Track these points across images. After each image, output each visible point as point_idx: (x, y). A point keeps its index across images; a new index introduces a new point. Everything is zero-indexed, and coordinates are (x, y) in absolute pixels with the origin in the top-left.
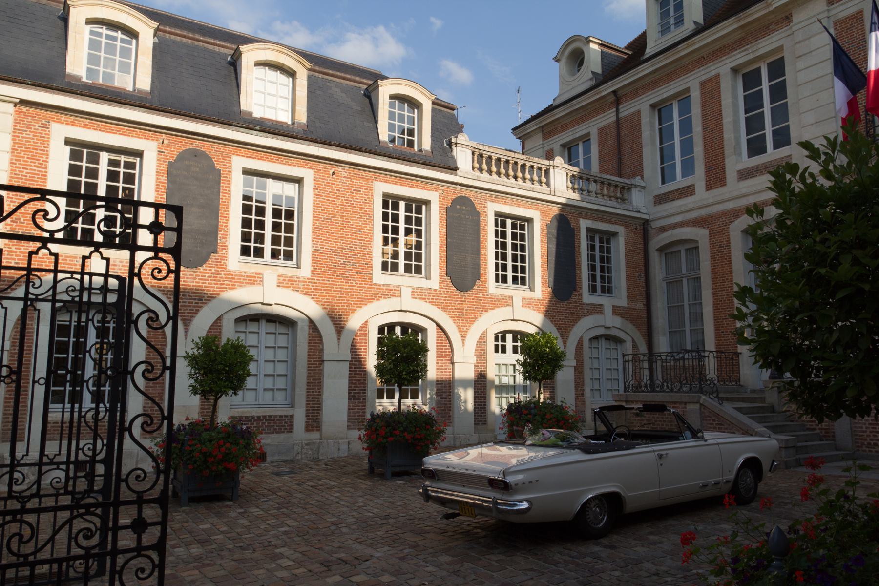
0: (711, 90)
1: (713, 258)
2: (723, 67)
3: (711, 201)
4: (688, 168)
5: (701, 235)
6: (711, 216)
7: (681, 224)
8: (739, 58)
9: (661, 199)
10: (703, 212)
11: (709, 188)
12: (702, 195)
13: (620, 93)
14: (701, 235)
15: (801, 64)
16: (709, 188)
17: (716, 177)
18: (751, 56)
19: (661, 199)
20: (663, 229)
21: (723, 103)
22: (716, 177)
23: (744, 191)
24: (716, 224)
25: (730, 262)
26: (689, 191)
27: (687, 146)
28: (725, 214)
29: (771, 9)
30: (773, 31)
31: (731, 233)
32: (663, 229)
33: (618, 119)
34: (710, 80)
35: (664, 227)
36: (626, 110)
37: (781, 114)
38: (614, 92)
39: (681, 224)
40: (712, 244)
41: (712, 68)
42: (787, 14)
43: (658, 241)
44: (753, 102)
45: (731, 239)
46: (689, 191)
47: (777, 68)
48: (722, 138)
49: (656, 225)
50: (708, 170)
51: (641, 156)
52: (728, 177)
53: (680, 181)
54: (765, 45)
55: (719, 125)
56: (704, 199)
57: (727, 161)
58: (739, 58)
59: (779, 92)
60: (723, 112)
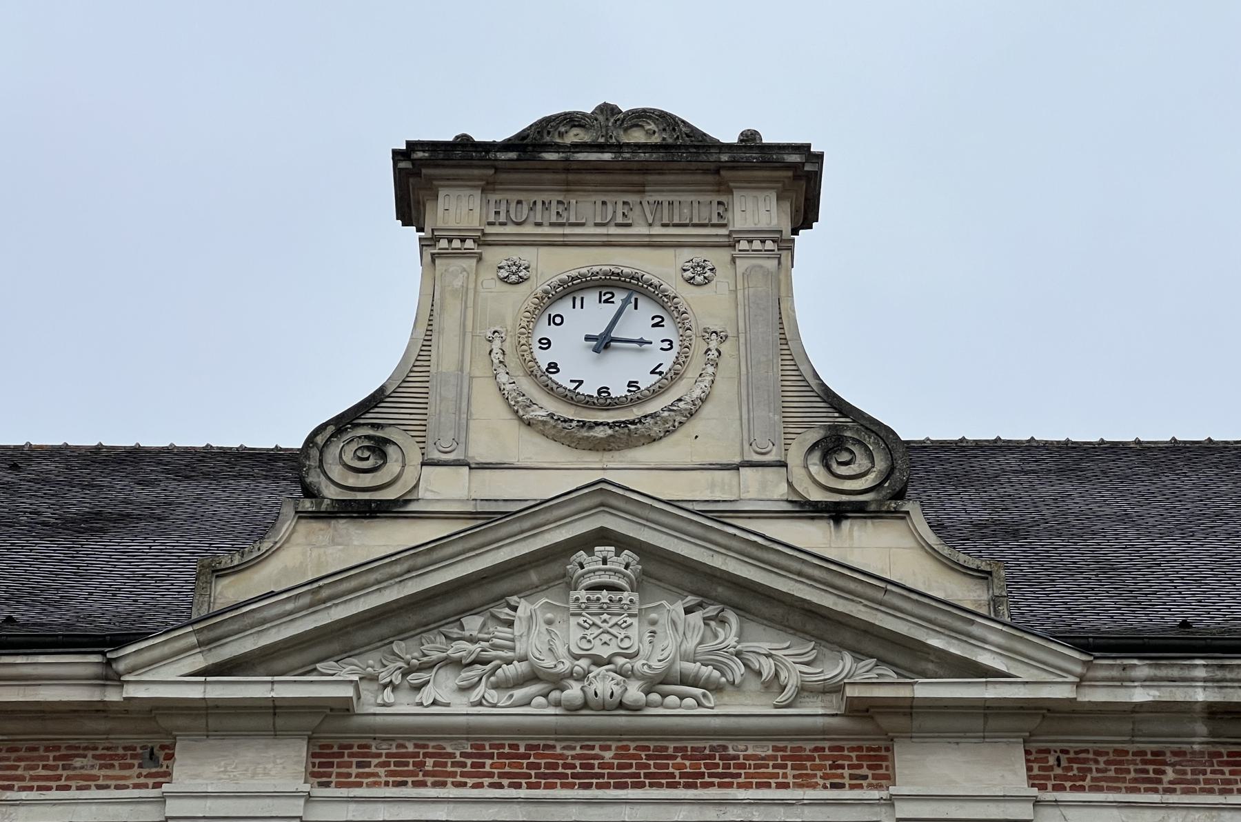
29: (113, 696)
42: (156, 742)
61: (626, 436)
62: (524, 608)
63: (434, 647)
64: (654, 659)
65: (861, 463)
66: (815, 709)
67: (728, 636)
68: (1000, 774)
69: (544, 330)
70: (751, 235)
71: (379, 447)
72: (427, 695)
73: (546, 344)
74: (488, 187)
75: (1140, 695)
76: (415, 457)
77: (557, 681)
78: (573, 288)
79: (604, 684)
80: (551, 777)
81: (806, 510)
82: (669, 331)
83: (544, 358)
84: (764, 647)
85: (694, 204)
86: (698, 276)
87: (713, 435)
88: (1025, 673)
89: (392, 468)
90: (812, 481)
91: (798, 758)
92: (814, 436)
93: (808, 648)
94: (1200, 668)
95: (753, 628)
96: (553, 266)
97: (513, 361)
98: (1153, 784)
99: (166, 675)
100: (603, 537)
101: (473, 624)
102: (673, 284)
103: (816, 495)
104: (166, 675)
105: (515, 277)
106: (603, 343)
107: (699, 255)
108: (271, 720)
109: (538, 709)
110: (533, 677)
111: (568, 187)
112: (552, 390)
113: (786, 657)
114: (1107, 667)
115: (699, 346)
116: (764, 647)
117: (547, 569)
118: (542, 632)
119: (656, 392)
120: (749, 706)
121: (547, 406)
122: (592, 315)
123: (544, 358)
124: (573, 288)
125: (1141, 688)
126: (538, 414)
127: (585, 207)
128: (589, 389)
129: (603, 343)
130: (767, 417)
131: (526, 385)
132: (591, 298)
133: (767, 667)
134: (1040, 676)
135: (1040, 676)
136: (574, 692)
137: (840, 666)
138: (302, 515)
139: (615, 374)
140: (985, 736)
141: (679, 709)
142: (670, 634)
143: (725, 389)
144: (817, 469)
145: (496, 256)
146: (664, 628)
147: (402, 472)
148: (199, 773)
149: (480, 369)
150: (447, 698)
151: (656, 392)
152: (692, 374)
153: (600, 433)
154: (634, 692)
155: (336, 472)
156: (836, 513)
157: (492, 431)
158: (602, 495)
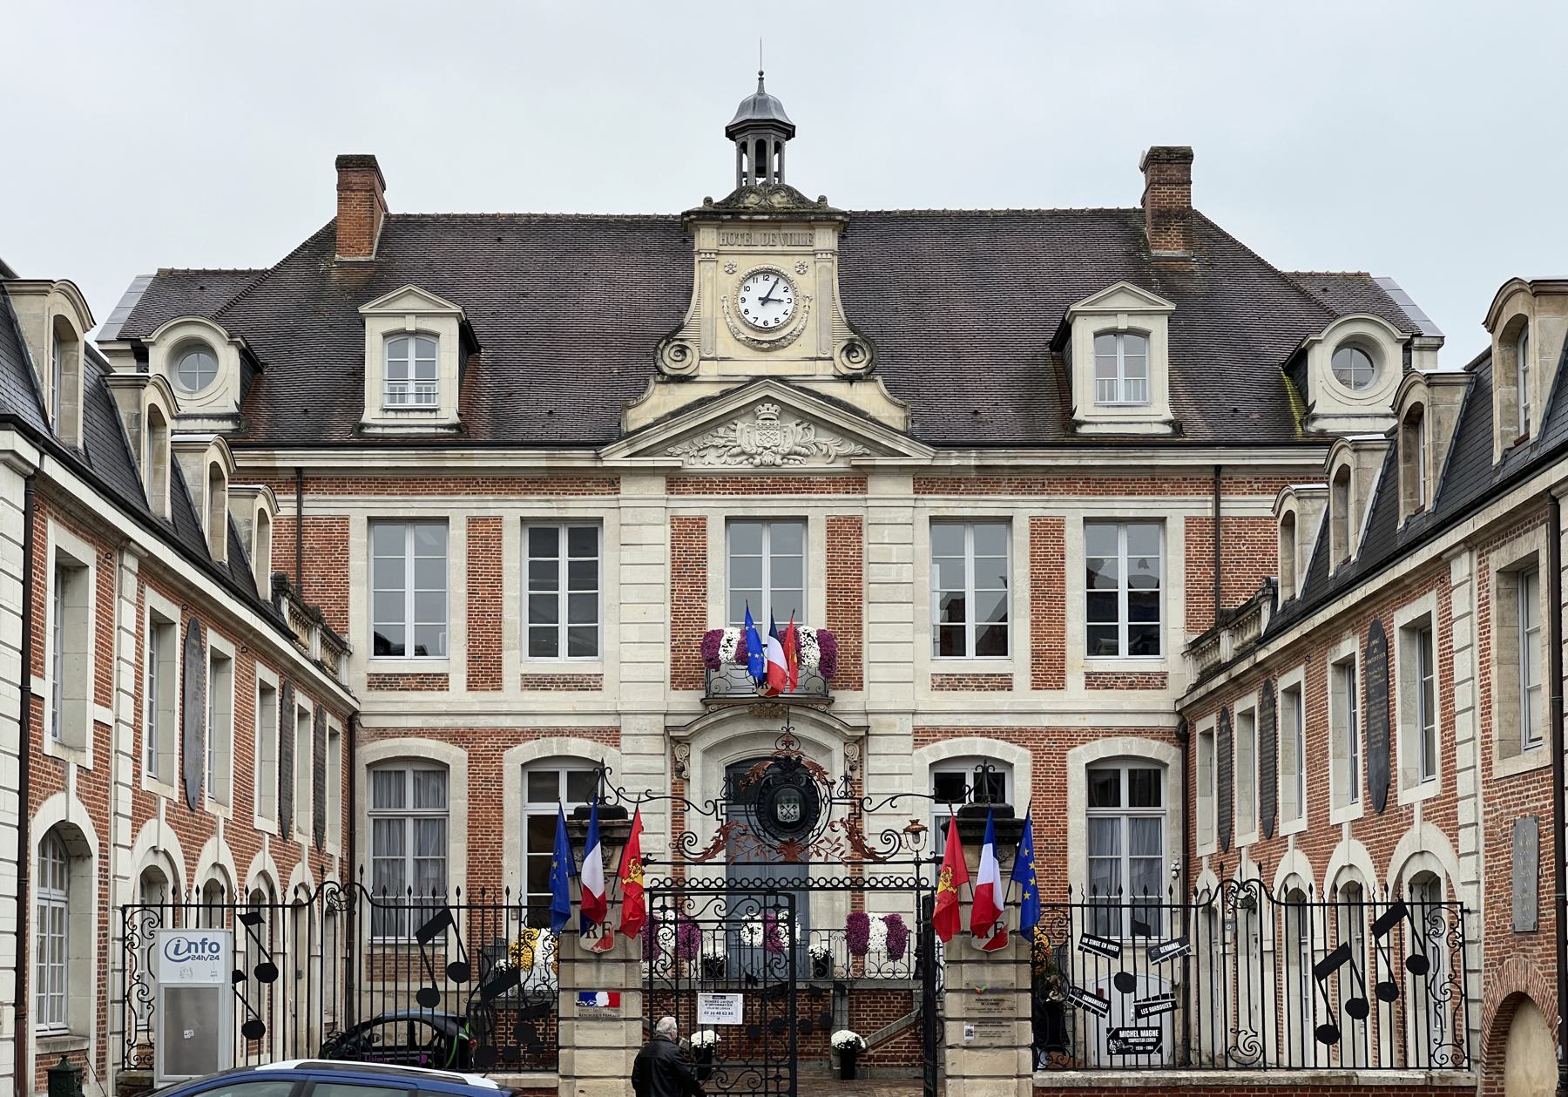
0: (484, 536)
1: (472, 796)
2: (512, 511)
3: (477, 708)
5: (455, 757)
6: (473, 731)
7: (419, 732)
8: (540, 506)
9: (380, 682)
10: (461, 722)
11: (471, 686)
12: (458, 695)
13: (306, 474)
14: (455, 757)
15: (628, 555)
16: (471, 686)
17: (485, 672)
19: (380, 682)
20: (383, 733)
21: (505, 564)
22: (485, 672)
23: (532, 708)
24: (484, 746)
26: (438, 682)
28: (498, 732)
29: (599, 464)
31: (505, 765)
32: (383, 733)
33: (300, 516)
34: (485, 519)
35: (385, 729)
36: (319, 506)
37: (586, 608)
38: (299, 470)
39: (419, 732)
40: (473, 775)
41: (491, 504)
43: (369, 752)
44: (542, 576)
45: (505, 773)
46: (438, 682)
49: (366, 722)
50: (473, 658)
51: (346, 597)
52: (505, 678)
54: (579, 506)
55: (497, 596)
57: (505, 655)
58: (540, 506)
59: (585, 576)
60: (505, 579)
61: (774, 346)
62: (740, 425)
63: (709, 441)
65: (861, 356)
66: (840, 465)
68: (903, 488)
69: (743, 294)
70: (822, 251)
71: (683, 350)
72: (706, 460)
73: (744, 300)
74: (718, 228)
75: (954, 463)
76: (697, 355)
77: (752, 456)
78: (753, 275)
79: (768, 458)
80: (749, 490)
81: (842, 378)
82: (790, 294)
83: (743, 307)
84: (823, 440)
85: (799, 233)
87: (806, 345)
88: (914, 455)
89: (689, 359)
90: (843, 365)
91: (834, 482)
92: (844, 344)
93: (839, 440)
94: (973, 453)
95: (820, 431)
97: (732, 311)
98: (955, 491)
99: (616, 457)
100: (768, 399)
101: (721, 430)
102: (792, 275)
103: (845, 371)
104: (616, 457)
105: (731, 271)
106: (765, 301)
107: (802, 259)
108: (654, 471)
109: (746, 466)
110: (743, 453)
111: (751, 227)
112: (747, 324)
114: (943, 453)
115: (802, 303)
116: (823, 440)
118: (747, 435)
122: (761, 287)
123: (743, 307)
124: (753, 275)
125: (954, 459)
126: (742, 337)
127: (757, 236)
128: (760, 323)
129: (765, 301)
130: (826, 337)
131: (737, 322)
132: (760, 278)
133: (825, 448)
134: (920, 456)
135: (920, 456)
136: (757, 461)
137: (850, 448)
138: (657, 382)
139: (770, 315)
140: (899, 475)
141: (793, 465)
142: (790, 436)
143: (811, 324)
144: (844, 359)
145: (723, 259)
146: (789, 435)
147: (690, 364)
148: (628, 489)
149: (720, 315)
151: (786, 325)
152: (799, 317)
153: (765, 346)
154: (778, 461)
155: (667, 361)
156: (851, 379)
157: (726, 345)
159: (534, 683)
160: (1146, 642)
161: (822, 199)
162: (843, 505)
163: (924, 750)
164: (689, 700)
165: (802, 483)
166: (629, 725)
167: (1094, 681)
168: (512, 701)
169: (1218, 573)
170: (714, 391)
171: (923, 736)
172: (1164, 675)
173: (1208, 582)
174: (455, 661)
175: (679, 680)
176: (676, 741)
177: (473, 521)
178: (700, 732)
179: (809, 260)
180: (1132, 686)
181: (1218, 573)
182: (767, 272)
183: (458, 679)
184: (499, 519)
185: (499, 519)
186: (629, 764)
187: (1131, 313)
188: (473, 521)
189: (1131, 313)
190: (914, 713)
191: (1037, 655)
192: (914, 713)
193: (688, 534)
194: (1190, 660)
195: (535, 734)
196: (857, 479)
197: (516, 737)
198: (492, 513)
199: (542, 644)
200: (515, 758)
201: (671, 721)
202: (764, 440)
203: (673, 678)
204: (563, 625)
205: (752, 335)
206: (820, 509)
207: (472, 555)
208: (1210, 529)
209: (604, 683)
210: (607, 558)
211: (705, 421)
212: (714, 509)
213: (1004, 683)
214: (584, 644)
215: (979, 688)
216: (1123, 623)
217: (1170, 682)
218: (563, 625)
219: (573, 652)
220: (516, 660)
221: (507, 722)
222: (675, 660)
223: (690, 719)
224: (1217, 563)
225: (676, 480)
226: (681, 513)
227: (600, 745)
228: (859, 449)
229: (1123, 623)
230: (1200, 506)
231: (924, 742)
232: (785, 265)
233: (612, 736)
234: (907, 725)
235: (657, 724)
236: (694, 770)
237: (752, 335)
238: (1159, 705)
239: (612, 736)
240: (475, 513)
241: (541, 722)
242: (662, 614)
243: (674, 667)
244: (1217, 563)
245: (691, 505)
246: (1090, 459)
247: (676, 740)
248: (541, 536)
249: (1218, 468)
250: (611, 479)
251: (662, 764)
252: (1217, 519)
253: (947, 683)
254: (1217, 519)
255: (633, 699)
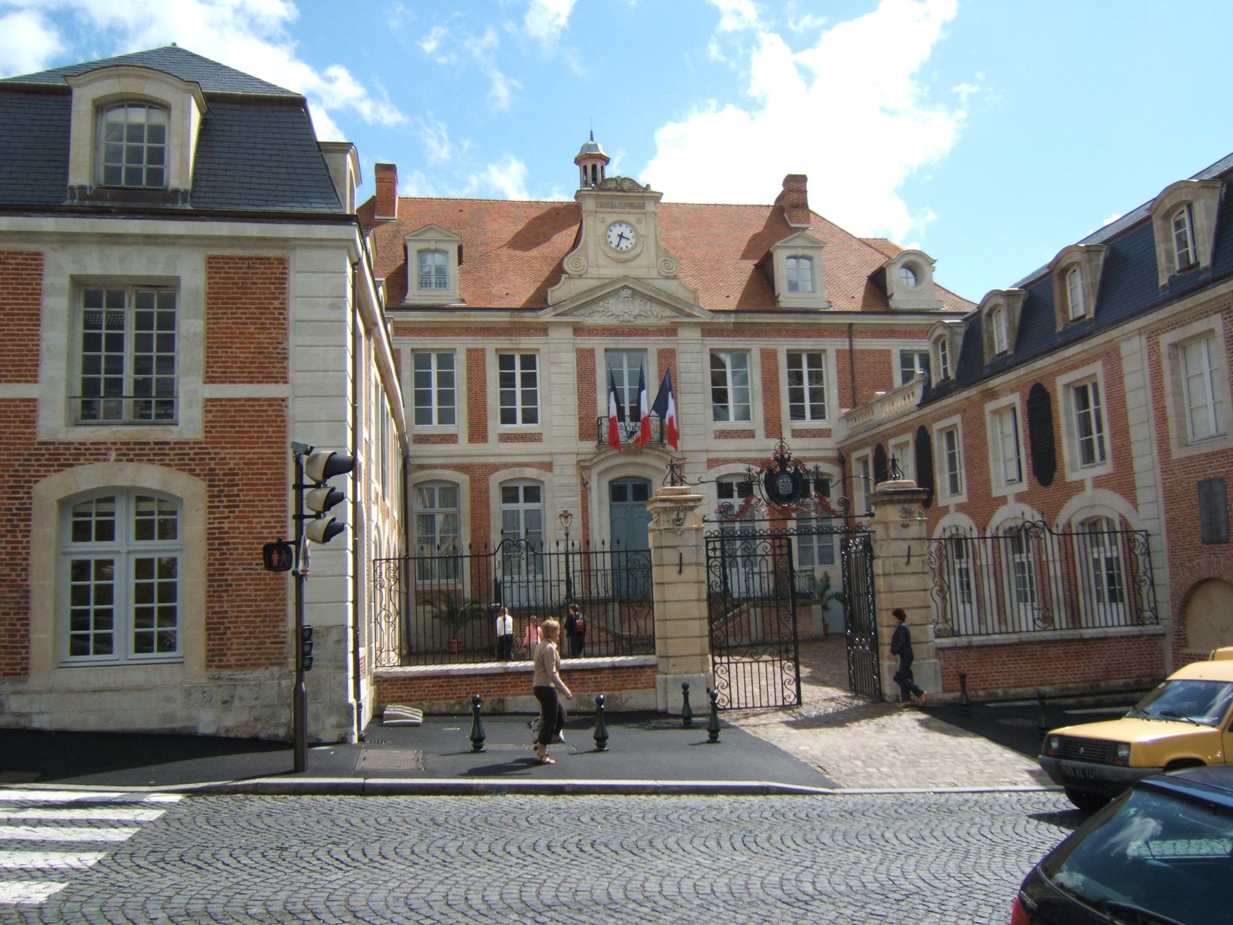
1: (473, 501)
3: (474, 453)
4: (447, 417)
5: (463, 479)
8: (504, 343)
10: (466, 461)
11: (471, 440)
14: (463, 479)
16: (471, 440)
17: (478, 433)
18: (514, 347)
20: (422, 467)
22: (478, 433)
23: (505, 452)
24: (478, 473)
25: (488, 506)
26: (451, 439)
27: (446, 398)
28: (486, 465)
30: (533, 335)
37: (530, 398)
40: (472, 488)
46: (451, 439)
47: (529, 361)
48: (485, 403)
50: (472, 425)
53: (435, 427)
54: (528, 343)
56: (464, 448)
59: (529, 380)
61: (627, 261)
64: (636, 312)
66: (664, 322)
67: (648, 306)
68: (696, 334)
79: (627, 318)
86: (639, 221)
87: (642, 261)
93: (662, 309)
96: (610, 218)
99: (546, 316)
100: (626, 287)
105: (603, 221)
108: (566, 324)
113: (657, 309)
117: (615, 293)
119: (632, 249)
120: (652, 321)
121: (612, 254)
122: (617, 230)
124: (614, 224)
129: (621, 236)
137: (668, 313)
141: (641, 322)
142: (637, 307)
145: (599, 216)
148: (553, 333)
150: (597, 320)
151: (632, 249)
157: (602, 260)
158: (625, 278)
159: (506, 438)
160: (818, 413)
161: (648, 186)
162: (664, 343)
163: (713, 470)
164: (590, 446)
165: (644, 332)
166: (558, 460)
167: (796, 434)
168: (493, 449)
169: (853, 378)
170: (595, 283)
171: (712, 463)
172: (829, 430)
173: (848, 382)
174: (460, 426)
175: (584, 435)
176: (584, 468)
177: (469, 351)
178: (596, 464)
179: (643, 217)
180: (814, 436)
181: (853, 378)
182: (621, 223)
183: (463, 436)
184: (483, 350)
185: (483, 350)
186: (557, 481)
187: (804, 248)
188: (469, 351)
189: (804, 248)
190: (707, 451)
191: (767, 420)
192: (707, 451)
193: (585, 358)
194: (844, 422)
195: (506, 466)
196: (671, 330)
197: (496, 468)
198: (480, 346)
199: (508, 417)
200: (495, 480)
201: (580, 458)
202: (620, 310)
203: (580, 435)
204: (519, 407)
205: (615, 255)
206: (653, 345)
207: (469, 369)
208: (848, 356)
209: (544, 438)
210: (540, 371)
211: (592, 300)
212: (599, 344)
213: (750, 434)
214: (530, 417)
215: (739, 437)
216: (807, 404)
217: (833, 433)
218: (519, 407)
219: (525, 421)
220: (496, 427)
221: (492, 460)
222: (581, 425)
223: (590, 457)
224: (852, 373)
225: (578, 330)
226: (581, 346)
227: (542, 472)
228: (674, 314)
229: (807, 404)
230: (843, 344)
231: (713, 467)
232: (632, 219)
233: (548, 466)
234: (704, 457)
235: (574, 459)
236: (594, 483)
237: (615, 255)
238: (827, 446)
239: (548, 466)
240: (471, 346)
241: (509, 460)
242: (572, 400)
243: (580, 429)
244: (852, 373)
245: (587, 342)
246: (789, 319)
247: (583, 468)
248: (506, 361)
249: (851, 325)
250: (543, 329)
251: (575, 480)
252: (851, 351)
253: (723, 435)
254: (851, 351)
255: (558, 447)
